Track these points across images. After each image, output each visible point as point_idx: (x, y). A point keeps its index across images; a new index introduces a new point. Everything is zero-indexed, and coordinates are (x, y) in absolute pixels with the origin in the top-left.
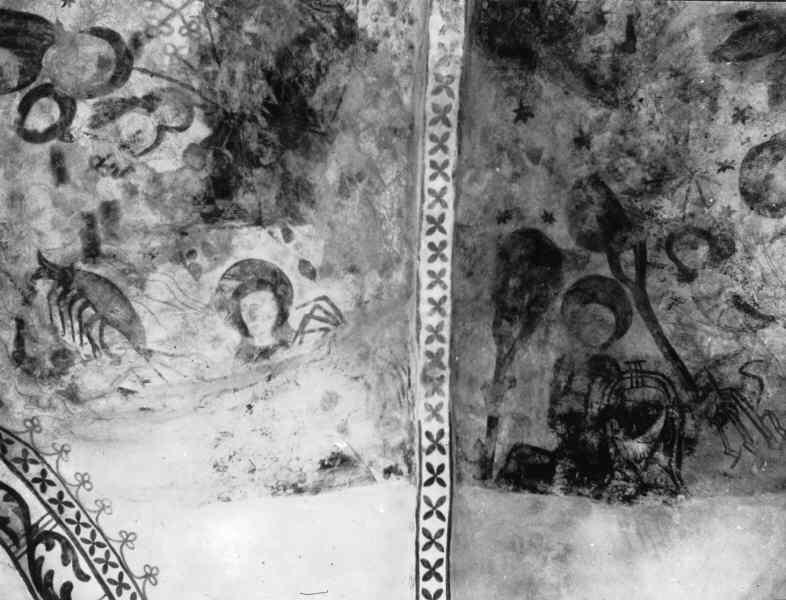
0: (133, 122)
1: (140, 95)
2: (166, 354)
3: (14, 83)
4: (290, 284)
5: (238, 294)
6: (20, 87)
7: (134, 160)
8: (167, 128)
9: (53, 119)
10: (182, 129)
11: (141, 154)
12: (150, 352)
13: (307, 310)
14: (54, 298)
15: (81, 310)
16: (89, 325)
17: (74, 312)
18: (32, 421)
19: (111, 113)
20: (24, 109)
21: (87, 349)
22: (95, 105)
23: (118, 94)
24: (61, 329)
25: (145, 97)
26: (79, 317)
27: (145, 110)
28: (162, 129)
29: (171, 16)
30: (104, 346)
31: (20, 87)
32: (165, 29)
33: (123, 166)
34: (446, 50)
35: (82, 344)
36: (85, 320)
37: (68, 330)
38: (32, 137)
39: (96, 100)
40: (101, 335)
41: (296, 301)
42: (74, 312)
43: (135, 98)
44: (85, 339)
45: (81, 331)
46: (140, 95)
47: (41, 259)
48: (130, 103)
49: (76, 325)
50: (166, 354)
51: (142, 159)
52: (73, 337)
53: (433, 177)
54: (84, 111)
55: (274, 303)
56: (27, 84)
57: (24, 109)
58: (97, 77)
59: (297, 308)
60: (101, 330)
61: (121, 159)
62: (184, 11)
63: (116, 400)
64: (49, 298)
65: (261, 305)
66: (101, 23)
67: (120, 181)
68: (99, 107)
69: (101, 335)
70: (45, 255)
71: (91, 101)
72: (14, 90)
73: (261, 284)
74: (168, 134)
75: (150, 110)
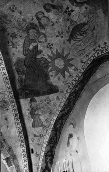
0: (43, 21)
3: (36, 44)
6: (37, 43)
7: (51, 21)
8: (44, 16)
10: (43, 13)
11: (49, 20)
12: (87, 22)
14: (74, 40)
15: (77, 35)
16: (80, 33)
17: (77, 36)
19: (42, 27)
20: (40, 42)
26: (79, 35)
28: (44, 17)
30: (85, 31)
31: (37, 43)
35: (83, 36)
38: (46, 41)
39: (40, 29)
42: (77, 36)
43: (38, 22)
44: (83, 35)
45: (81, 36)
47: (68, 41)
48: (40, 24)
49: (80, 36)
51: (50, 20)
54: (43, 31)
60: (82, 31)
63: (95, 31)
64: (74, 41)
67: (55, 24)
68: (41, 28)
70: (67, 40)
72: (37, 44)
74: (45, 16)
75: (41, 19)
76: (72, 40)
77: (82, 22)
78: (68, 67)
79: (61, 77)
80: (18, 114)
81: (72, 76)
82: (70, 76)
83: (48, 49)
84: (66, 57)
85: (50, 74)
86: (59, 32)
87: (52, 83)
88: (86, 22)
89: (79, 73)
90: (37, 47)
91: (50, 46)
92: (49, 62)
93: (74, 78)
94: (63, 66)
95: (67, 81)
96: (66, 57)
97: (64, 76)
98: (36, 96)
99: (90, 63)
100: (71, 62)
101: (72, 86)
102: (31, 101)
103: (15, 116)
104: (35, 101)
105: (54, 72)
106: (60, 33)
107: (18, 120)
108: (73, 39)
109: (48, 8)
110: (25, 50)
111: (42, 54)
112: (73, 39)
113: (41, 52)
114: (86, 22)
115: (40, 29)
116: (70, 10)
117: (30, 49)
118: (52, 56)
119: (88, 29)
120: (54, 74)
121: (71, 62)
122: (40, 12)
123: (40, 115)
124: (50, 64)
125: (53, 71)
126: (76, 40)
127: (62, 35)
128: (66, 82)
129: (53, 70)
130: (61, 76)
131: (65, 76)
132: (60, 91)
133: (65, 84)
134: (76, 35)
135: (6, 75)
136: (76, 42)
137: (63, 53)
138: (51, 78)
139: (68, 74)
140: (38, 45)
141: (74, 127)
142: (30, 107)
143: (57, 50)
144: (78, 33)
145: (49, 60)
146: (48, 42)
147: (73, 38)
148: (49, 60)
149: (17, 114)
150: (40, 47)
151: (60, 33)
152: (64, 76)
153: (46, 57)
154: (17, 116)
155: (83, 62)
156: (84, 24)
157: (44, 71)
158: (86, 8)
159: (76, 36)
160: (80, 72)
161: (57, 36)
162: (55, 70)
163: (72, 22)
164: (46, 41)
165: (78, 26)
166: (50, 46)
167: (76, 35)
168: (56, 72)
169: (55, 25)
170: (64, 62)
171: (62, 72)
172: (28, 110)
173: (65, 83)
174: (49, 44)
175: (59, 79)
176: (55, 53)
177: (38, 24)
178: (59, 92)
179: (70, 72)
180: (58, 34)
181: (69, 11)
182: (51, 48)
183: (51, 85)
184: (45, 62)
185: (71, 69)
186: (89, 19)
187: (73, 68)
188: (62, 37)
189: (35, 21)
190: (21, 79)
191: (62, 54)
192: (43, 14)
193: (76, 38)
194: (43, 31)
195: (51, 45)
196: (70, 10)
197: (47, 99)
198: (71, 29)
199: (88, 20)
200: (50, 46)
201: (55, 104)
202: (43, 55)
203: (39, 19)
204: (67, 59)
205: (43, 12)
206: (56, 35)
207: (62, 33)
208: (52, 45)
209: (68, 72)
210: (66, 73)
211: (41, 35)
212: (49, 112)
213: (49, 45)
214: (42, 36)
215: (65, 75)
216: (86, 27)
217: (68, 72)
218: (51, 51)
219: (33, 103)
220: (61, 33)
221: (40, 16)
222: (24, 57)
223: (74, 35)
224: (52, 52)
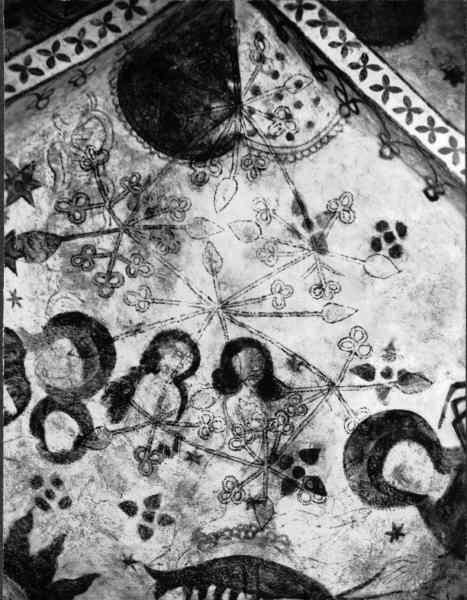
0: (146, 395)
1: (136, 363)
4: (412, 413)
5: (375, 470)
6: (20, 410)
9: (71, 430)
10: (195, 365)
11: (179, 417)
13: (450, 416)
19: (120, 399)
20: (37, 429)
22: (103, 398)
23: (119, 372)
25: (142, 362)
27: (151, 375)
28: (179, 381)
29: (111, 264)
32: (114, 281)
33: (170, 441)
34: (339, 44)
38: (62, 458)
39: (101, 392)
41: (433, 422)
43: (133, 368)
46: (136, 363)
48: (135, 376)
53: (432, 139)
55: (415, 446)
56: (25, 404)
57: (37, 429)
58: (87, 370)
59: (440, 427)
61: (161, 437)
62: (121, 250)
65: (406, 460)
66: (58, 309)
68: (109, 399)
70: (156, 568)
73: (386, 445)
74: (188, 381)
75: (155, 370)
86: (153, 501)
109: (241, 361)
115: (101, 392)
116: (310, 471)
122: (194, 348)
127: (154, 525)
143: (57, 547)
146: (65, 471)
147: (196, 592)
151: (158, 512)
158: (396, 533)
161: (129, 508)
163: (261, 528)
164: (62, 458)
166: (50, 494)
169: (167, 460)
174: (57, 482)
176: (38, 542)
177: (119, 372)
180: (142, 508)
181: (299, 472)
188: (146, 534)
189: (128, 355)
192: (187, 366)
194: (97, 409)
195: (59, 494)
196: (310, 471)
203: (150, 362)
205: (203, 361)
207: (166, 521)
214: (73, 424)
221: (169, 360)
223: (212, 588)
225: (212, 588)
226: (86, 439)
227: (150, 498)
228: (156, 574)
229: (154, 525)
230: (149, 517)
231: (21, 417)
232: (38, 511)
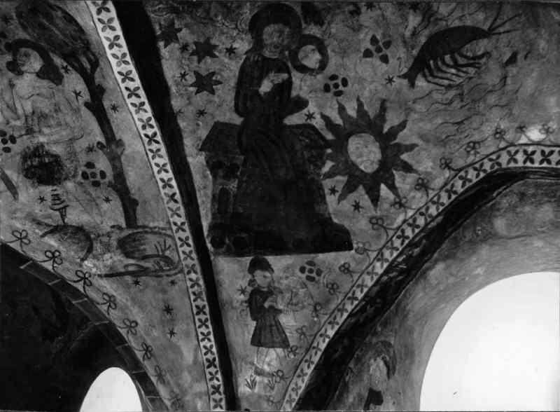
2: (495, 20)
3: (285, 76)
6: (289, 73)
16: (455, 61)
17: (444, 68)
18: (497, 133)
20: (303, 69)
21: (472, 71)
22: (306, 23)
24: (451, 83)
26: (448, 66)
30: (473, 58)
35: (466, 72)
36: (452, 63)
37: (454, 78)
38: (323, 65)
39: (303, 22)
40: (466, 57)
42: (444, 68)
44: (464, 69)
47: (404, 76)
49: (453, 71)
50: (495, 20)
52: (460, 76)
57: (303, 69)
64: (429, 82)
69: (466, 57)
71: (304, 25)
72: (290, 78)
76: (423, 79)
77: (469, 23)
78: (394, 172)
79: (365, 201)
80: (207, 307)
81: (405, 207)
82: (397, 206)
83: (329, 95)
84: (394, 132)
85: (327, 184)
86: (374, 40)
87: (331, 218)
88: (486, 28)
89: (430, 204)
90: (288, 84)
91: (336, 86)
92: (328, 144)
93: (410, 213)
94: (376, 166)
95: (384, 218)
96: (394, 132)
97: (375, 199)
98: (271, 254)
99: (475, 180)
100: (405, 157)
101: (399, 241)
102: (254, 266)
103: (198, 313)
104: (267, 267)
105: (341, 180)
106: (381, 44)
107: (207, 327)
108: (425, 76)
110: (245, 95)
111: (305, 111)
112: (427, 74)
113: (301, 104)
114: (486, 28)
115: (303, 22)
117: (262, 93)
118: (339, 121)
119: (487, 54)
120: (339, 188)
121: (405, 157)
123: (280, 311)
124: (329, 151)
125: (339, 178)
126: (436, 80)
127: (385, 51)
128: (380, 222)
129: (339, 174)
130: (366, 197)
131: (378, 200)
132: (355, 246)
133: (376, 226)
134: (440, 63)
135: (171, 186)
136: (438, 87)
137: (381, 116)
138: (331, 200)
139: (392, 197)
140: (294, 79)
141: (388, 373)
142: (249, 284)
143: (360, 105)
144: (447, 58)
145: (330, 137)
146: (330, 70)
147: (426, 70)
148: (330, 137)
149: (204, 306)
150: (301, 85)
151: (381, 44)
152: (375, 199)
153: (318, 122)
154: (205, 313)
155: (453, 165)
156: (475, 34)
157: (305, 173)
159: (439, 70)
160: (435, 199)
161: (368, 54)
162: (343, 175)
164: (323, 65)
165: (449, 31)
167: (440, 63)
168: (348, 181)
170: (383, 149)
171: (371, 184)
172: (243, 291)
173: (377, 223)
174: (333, 77)
175: (357, 206)
176: (352, 111)
178: (353, 252)
179: (399, 191)
180: (372, 48)
182: (339, 94)
183: (327, 222)
184: (311, 140)
185: (404, 182)
186: (499, 22)
187: (411, 178)
188: (385, 59)
190: (224, 192)
191: (378, 122)
193: (435, 74)
194: (313, 30)
195: (339, 81)
197: (308, 267)
198: (423, 40)
199: (491, 26)
200: (335, 86)
201: (335, 286)
202: (310, 116)
204: (392, 143)
206: (363, 50)
207: (388, 44)
208: (345, 83)
209: (392, 187)
210: (384, 189)
211: (305, 44)
212: (311, 308)
213: (331, 83)
214: (310, 47)
215: (379, 196)
216: (482, 46)
217: (392, 187)
218: (337, 106)
219: (259, 274)
220: (383, 44)
222: (238, 120)
223: (431, 62)
224: (342, 109)
225: (431, 62)
226: (321, 47)
227: (371, 39)
228: (404, 76)
229: (385, 51)
230: (379, 50)
231: (292, 74)
232: (340, 98)
